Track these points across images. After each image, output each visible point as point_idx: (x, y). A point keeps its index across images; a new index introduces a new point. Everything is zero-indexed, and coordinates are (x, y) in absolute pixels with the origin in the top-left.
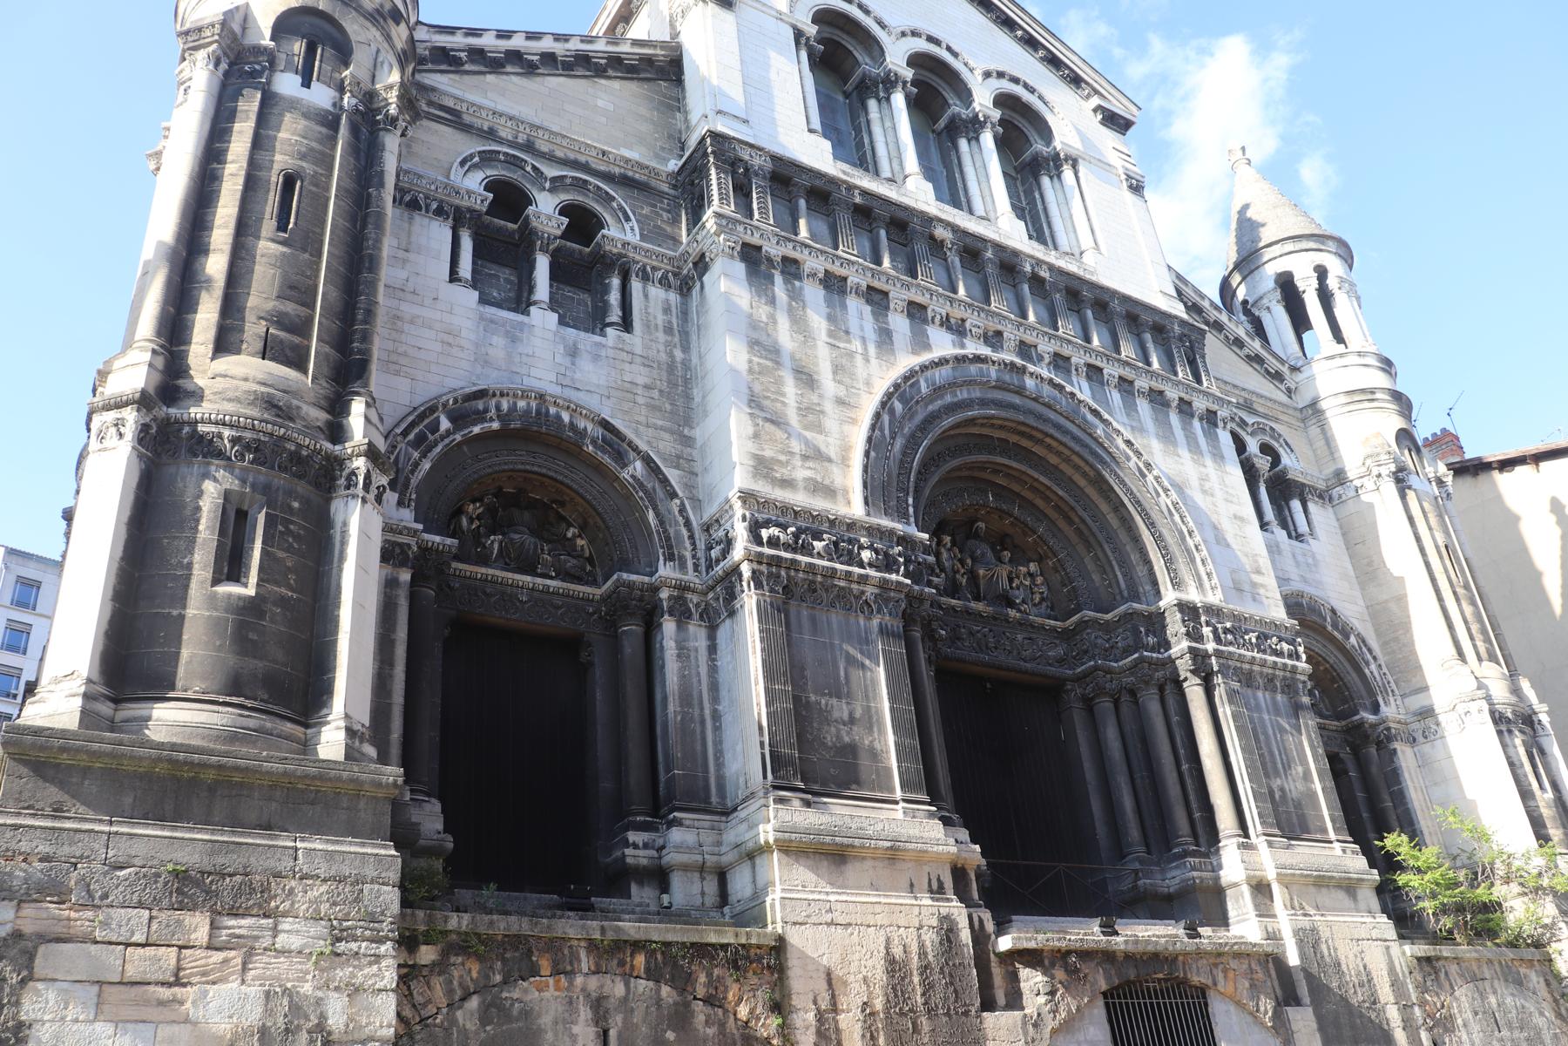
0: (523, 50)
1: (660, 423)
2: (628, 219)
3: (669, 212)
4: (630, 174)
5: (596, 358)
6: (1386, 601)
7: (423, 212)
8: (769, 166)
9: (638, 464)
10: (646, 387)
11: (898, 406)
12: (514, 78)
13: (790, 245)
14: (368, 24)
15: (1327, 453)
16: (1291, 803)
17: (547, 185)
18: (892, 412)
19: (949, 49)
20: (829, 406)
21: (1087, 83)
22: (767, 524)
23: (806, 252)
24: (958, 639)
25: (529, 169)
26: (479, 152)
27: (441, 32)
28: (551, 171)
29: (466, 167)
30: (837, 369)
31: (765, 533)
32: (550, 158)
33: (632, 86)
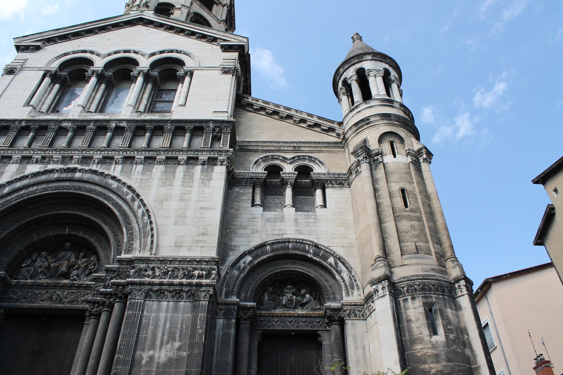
16: (155, 365)
21: (219, 39)
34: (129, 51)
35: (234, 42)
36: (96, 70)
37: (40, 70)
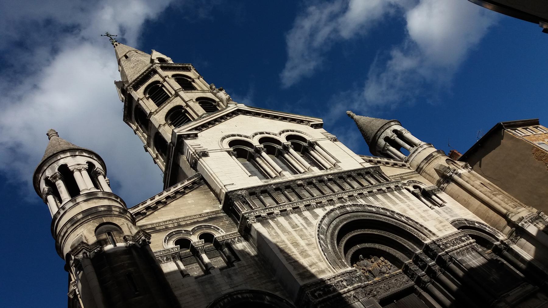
0: (160, 200)
1: (264, 281)
2: (219, 229)
3: (227, 220)
4: (211, 216)
5: (236, 274)
6: (477, 208)
7: (163, 262)
8: (247, 192)
9: (267, 297)
10: (254, 273)
11: (322, 236)
12: (162, 209)
13: (267, 210)
14: (120, 218)
15: (431, 178)
17: (191, 233)
18: (322, 239)
19: (267, 133)
20: (306, 248)
22: (315, 291)
23: (272, 209)
24: (378, 292)
25: (183, 232)
26: (167, 235)
27: (135, 208)
28: (190, 229)
29: (166, 242)
30: (301, 236)
31: (316, 294)
32: (187, 225)
33: (195, 192)
34: (262, 132)
35: (316, 122)
36: (260, 147)
37: (222, 151)
